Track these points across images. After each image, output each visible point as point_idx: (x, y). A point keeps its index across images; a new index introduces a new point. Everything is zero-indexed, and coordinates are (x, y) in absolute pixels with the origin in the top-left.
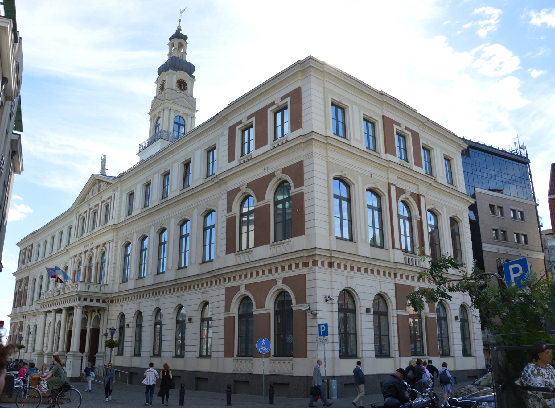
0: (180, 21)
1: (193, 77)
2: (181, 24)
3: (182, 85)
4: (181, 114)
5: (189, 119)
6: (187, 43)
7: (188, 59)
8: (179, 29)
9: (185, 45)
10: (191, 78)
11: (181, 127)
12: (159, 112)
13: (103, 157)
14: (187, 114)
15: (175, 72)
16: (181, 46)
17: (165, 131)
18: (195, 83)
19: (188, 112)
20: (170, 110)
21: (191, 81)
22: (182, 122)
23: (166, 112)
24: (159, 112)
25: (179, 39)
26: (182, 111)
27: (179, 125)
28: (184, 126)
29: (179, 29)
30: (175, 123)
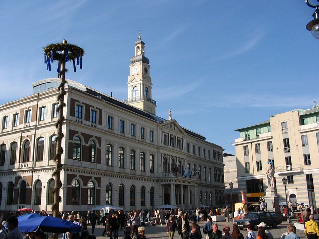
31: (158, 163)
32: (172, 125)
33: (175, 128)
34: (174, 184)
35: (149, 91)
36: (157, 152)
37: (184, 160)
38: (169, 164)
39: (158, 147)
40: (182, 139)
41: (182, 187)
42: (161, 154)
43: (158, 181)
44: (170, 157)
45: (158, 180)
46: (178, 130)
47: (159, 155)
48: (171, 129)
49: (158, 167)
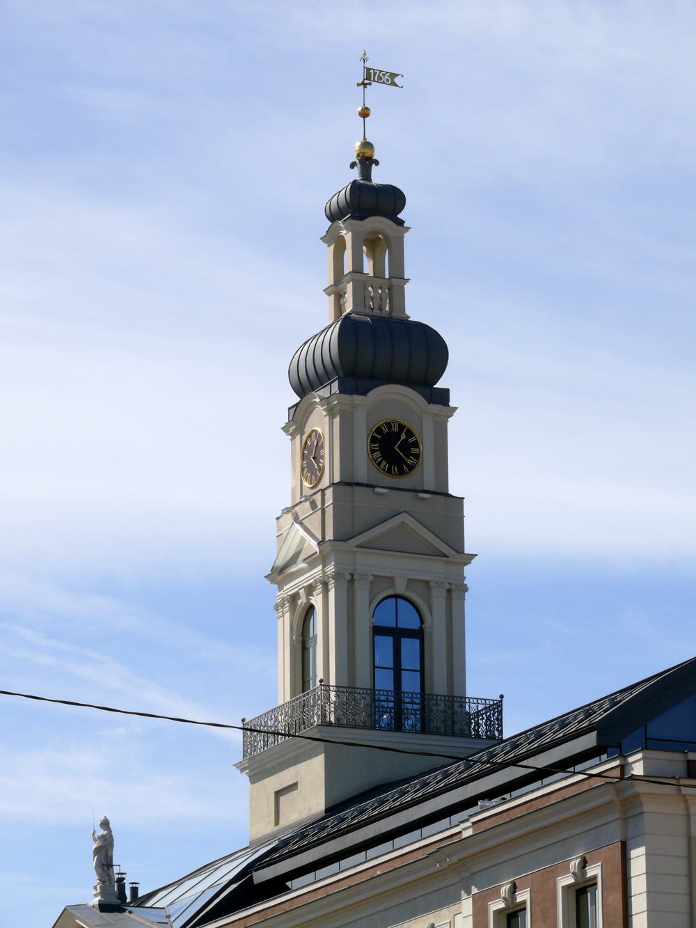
0: (365, 113)
1: (442, 397)
2: (376, 132)
4: (400, 588)
5: (439, 602)
8: (366, 161)
10: (435, 408)
13: (101, 832)
15: (358, 399)
18: (453, 425)
22: (409, 620)
24: (310, 590)
26: (403, 570)
27: (398, 634)
28: (419, 634)
29: (366, 161)
30: (378, 631)
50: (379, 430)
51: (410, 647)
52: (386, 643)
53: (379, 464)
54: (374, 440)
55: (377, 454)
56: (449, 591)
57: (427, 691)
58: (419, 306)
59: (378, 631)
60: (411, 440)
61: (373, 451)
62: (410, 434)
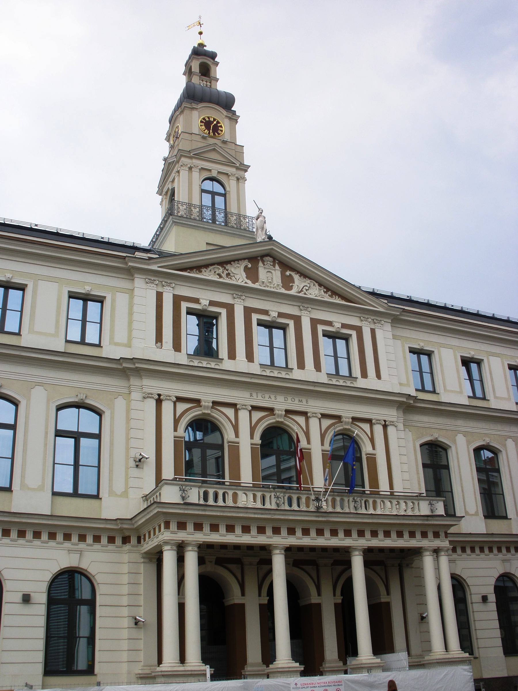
0: (201, 33)
2: (204, 40)
3: (212, 127)
4: (214, 174)
6: (217, 64)
7: (222, 86)
9: (212, 67)
11: (217, 197)
12: (173, 181)
14: (227, 174)
16: (206, 71)
17: (183, 204)
19: (231, 170)
20: (190, 168)
21: (230, 118)
23: (184, 174)
25: (203, 62)
27: (213, 194)
28: (224, 195)
31: (128, 448)
32: (262, 272)
33: (287, 282)
34: (181, 549)
35: (231, 185)
36: (126, 391)
37: (378, 429)
38: (235, 449)
39: (128, 369)
40: (359, 330)
41: (279, 564)
42: (152, 404)
43: (126, 540)
44: (244, 415)
45: (122, 534)
46: (315, 292)
47: (134, 405)
48: (256, 286)
49: (127, 468)
50: (204, 119)
51: (219, 200)
52: (207, 200)
53: (204, 130)
54: (201, 122)
55: (203, 127)
56: (238, 179)
57: (228, 210)
58: (223, 85)
59: (203, 191)
60: (219, 125)
61: (201, 126)
62: (218, 122)
